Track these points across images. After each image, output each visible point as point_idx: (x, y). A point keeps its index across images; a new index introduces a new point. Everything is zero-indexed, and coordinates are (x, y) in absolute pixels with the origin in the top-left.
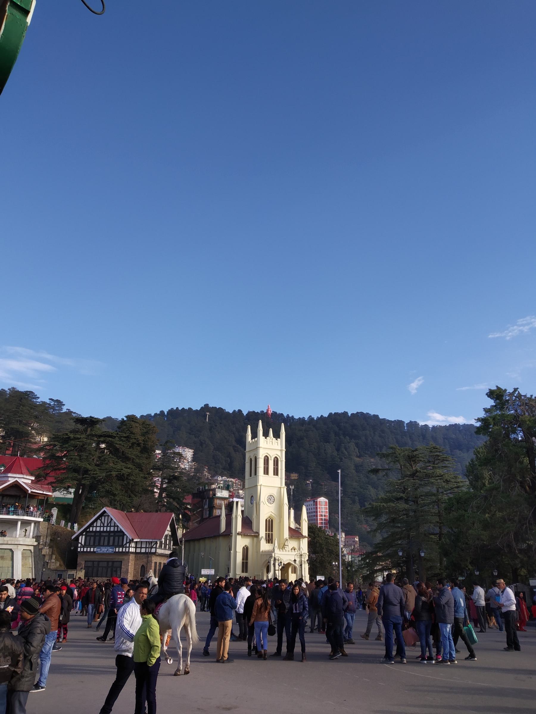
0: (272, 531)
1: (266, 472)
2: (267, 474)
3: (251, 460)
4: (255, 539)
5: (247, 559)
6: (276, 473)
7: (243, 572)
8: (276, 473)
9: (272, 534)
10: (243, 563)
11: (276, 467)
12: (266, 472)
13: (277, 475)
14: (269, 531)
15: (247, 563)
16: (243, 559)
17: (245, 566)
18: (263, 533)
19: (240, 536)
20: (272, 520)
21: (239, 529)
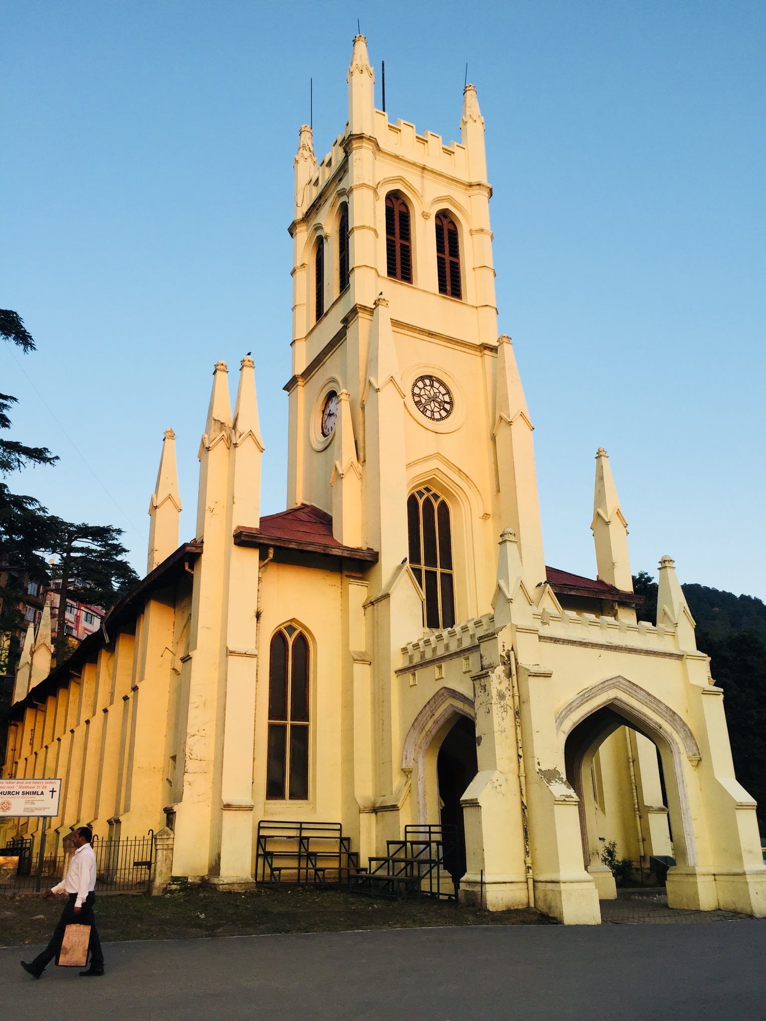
0: (447, 562)
1: (400, 266)
3: (320, 242)
5: (302, 710)
6: (450, 282)
7: (274, 791)
8: (450, 282)
9: (448, 579)
10: (276, 733)
11: (448, 258)
12: (400, 266)
14: (431, 561)
15: (301, 735)
16: (276, 710)
17: (288, 765)
18: (394, 547)
19: (252, 557)
20: (443, 505)
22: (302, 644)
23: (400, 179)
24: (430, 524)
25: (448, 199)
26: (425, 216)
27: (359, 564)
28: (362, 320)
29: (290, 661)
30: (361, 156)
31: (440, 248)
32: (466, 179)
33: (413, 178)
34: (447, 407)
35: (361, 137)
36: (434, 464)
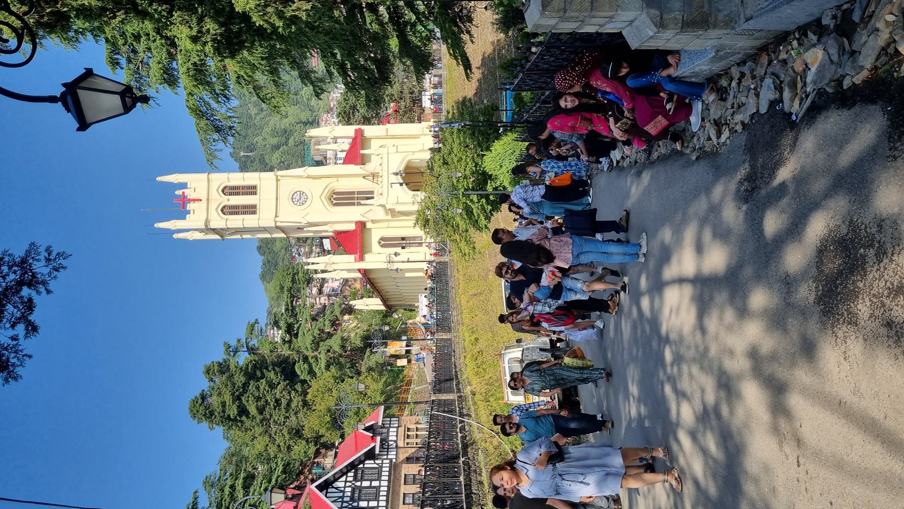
0: (353, 193)
1: (251, 210)
2: (254, 206)
4: (369, 225)
8: (251, 190)
9: (359, 193)
11: (241, 191)
13: (255, 187)
14: (353, 199)
21: (352, 258)
22: (382, 239)
23: (217, 209)
24: (341, 199)
25: (217, 190)
26: (228, 200)
27: (361, 225)
28: (279, 224)
29: (386, 242)
30: (213, 225)
31: (238, 194)
32: (206, 183)
33: (213, 206)
34: (302, 193)
35: (206, 226)
36: (323, 198)
